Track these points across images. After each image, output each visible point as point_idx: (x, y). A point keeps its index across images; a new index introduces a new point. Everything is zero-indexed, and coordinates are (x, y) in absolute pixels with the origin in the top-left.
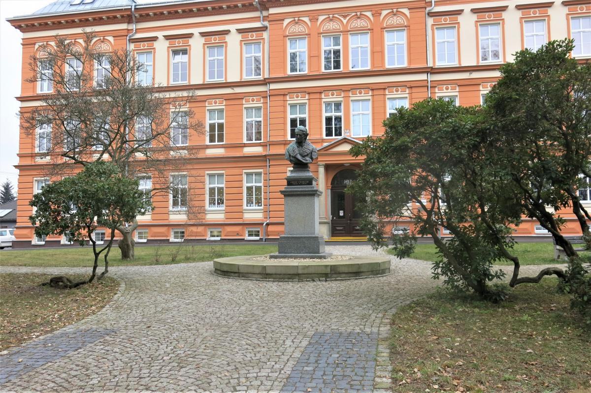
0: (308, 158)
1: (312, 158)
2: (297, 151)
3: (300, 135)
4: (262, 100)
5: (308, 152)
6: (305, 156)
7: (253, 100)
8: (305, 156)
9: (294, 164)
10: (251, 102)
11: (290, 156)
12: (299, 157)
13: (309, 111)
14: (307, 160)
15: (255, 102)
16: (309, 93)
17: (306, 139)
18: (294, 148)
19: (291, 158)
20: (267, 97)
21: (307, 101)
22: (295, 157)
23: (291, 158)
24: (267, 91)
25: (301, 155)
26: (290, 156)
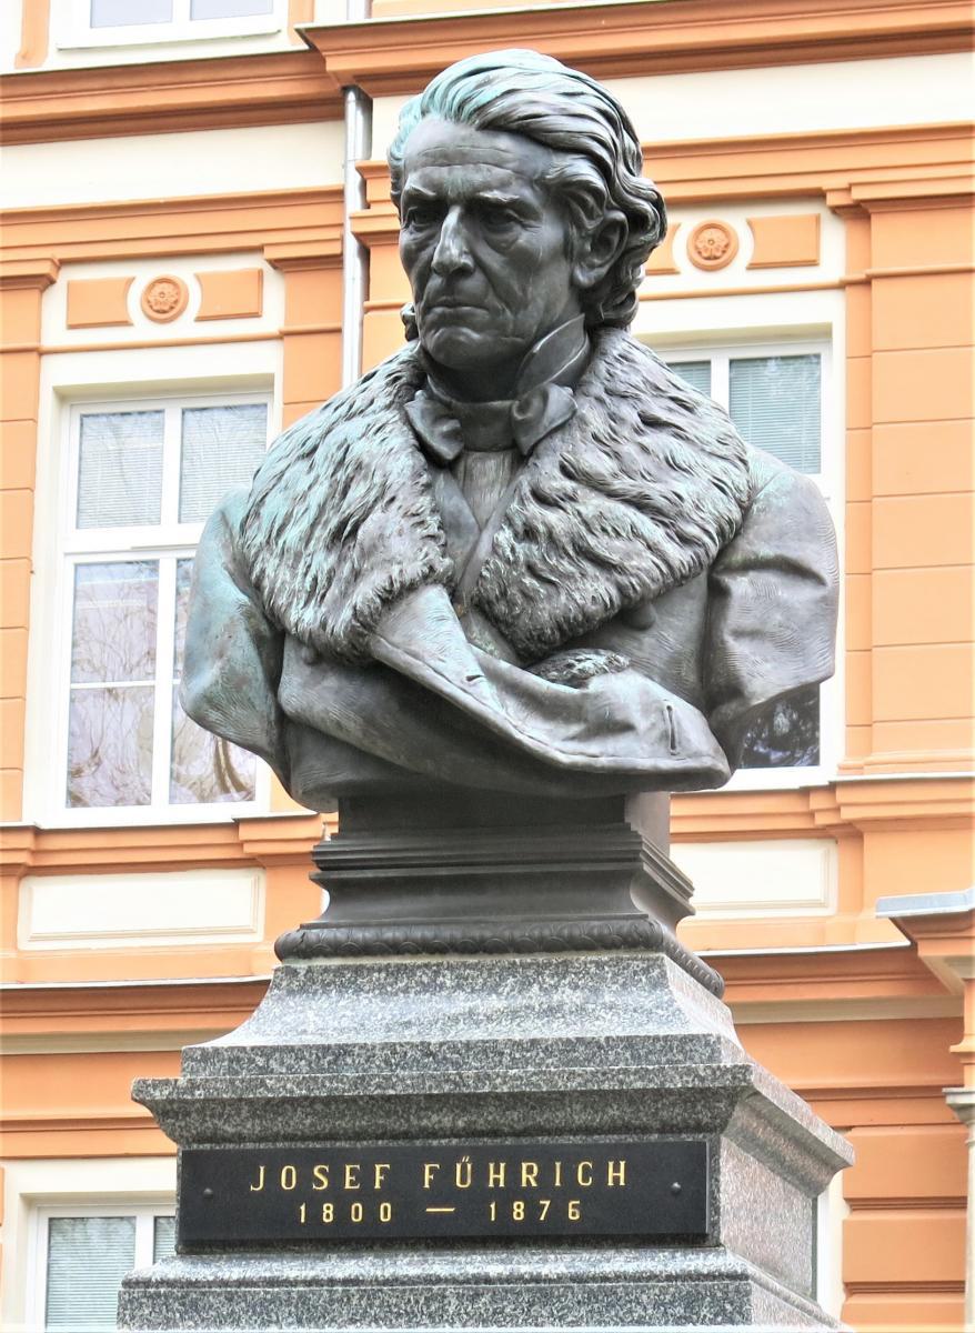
0: (623, 685)
1: (712, 687)
2: (403, 547)
3: (485, 215)
4: (276, 291)
5: (644, 553)
6: (583, 633)
7: (164, 308)
8: (583, 633)
9: (357, 806)
10: (144, 330)
11: (273, 636)
12: (445, 651)
13: (862, 427)
14: (611, 726)
15: (185, 327)
16: (858, 212)
17: (605, 307)
18: (348, 470)
19: (304, 691)
20: (335, 261)
21: (831, 310)
22: (355, 658)
23: (304, 691)
24: (337, 195)
25: (482, 608)
26: (273, 636)
